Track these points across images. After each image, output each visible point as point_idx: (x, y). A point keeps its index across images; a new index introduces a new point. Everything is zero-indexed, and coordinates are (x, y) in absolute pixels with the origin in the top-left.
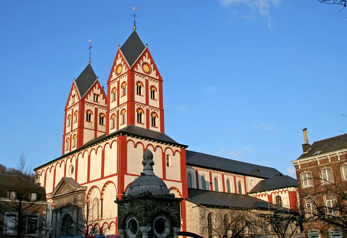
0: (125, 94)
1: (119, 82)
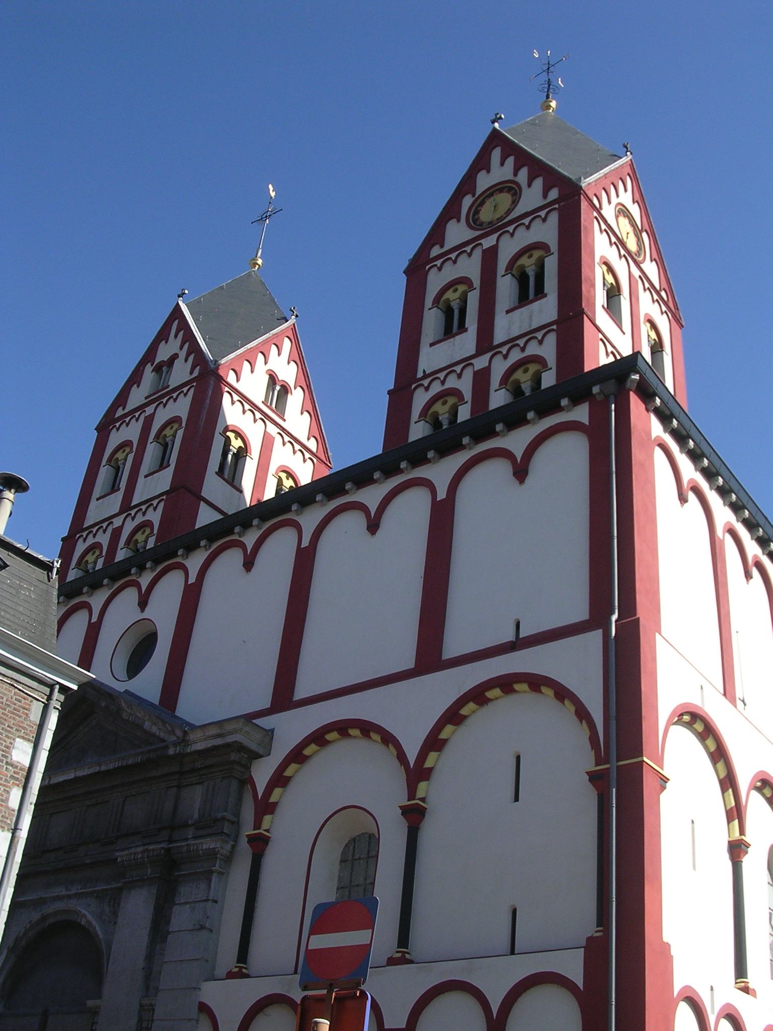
0: (165, 465)
1: (149, 421)
